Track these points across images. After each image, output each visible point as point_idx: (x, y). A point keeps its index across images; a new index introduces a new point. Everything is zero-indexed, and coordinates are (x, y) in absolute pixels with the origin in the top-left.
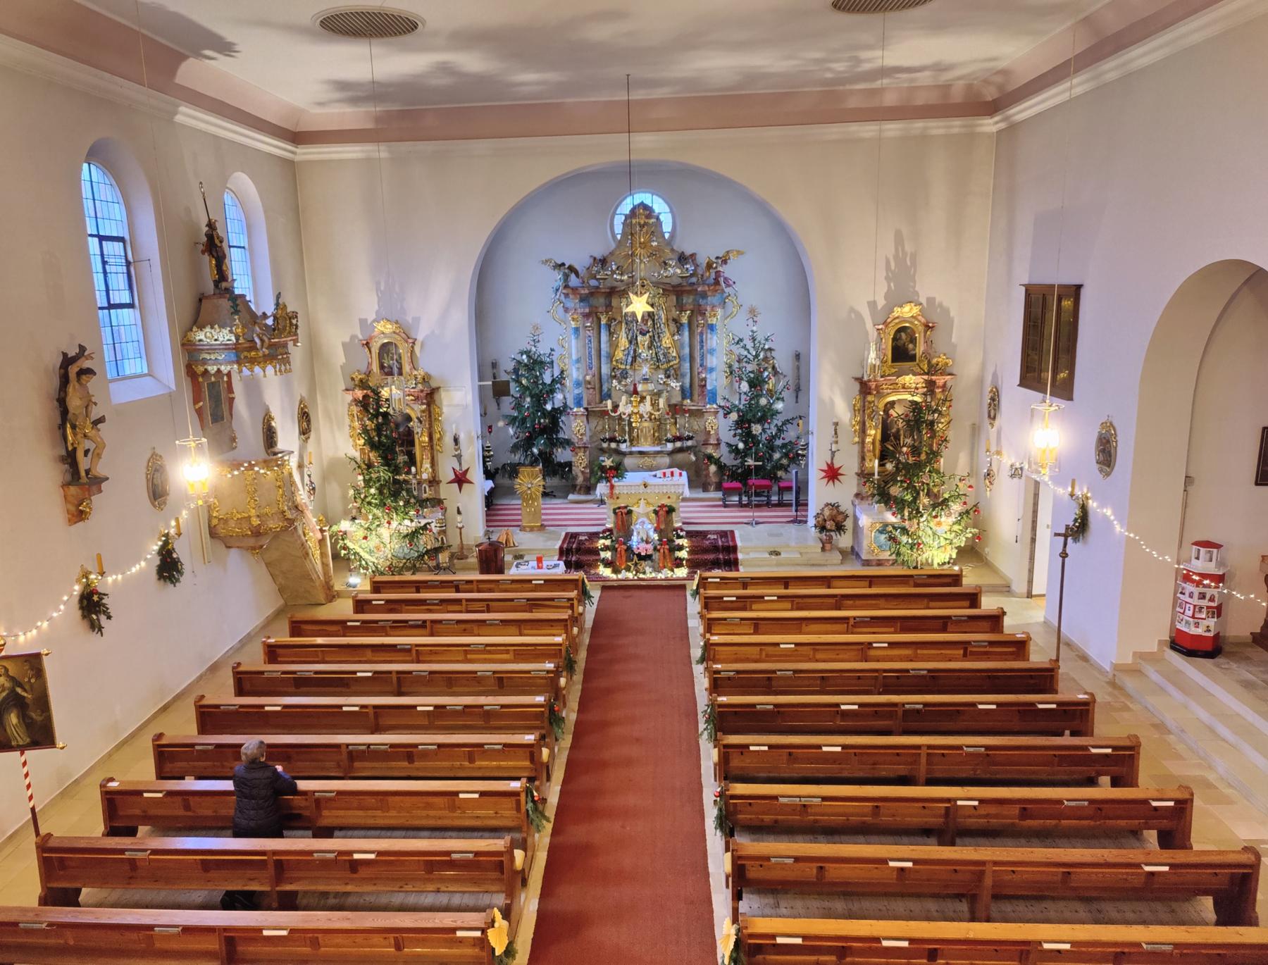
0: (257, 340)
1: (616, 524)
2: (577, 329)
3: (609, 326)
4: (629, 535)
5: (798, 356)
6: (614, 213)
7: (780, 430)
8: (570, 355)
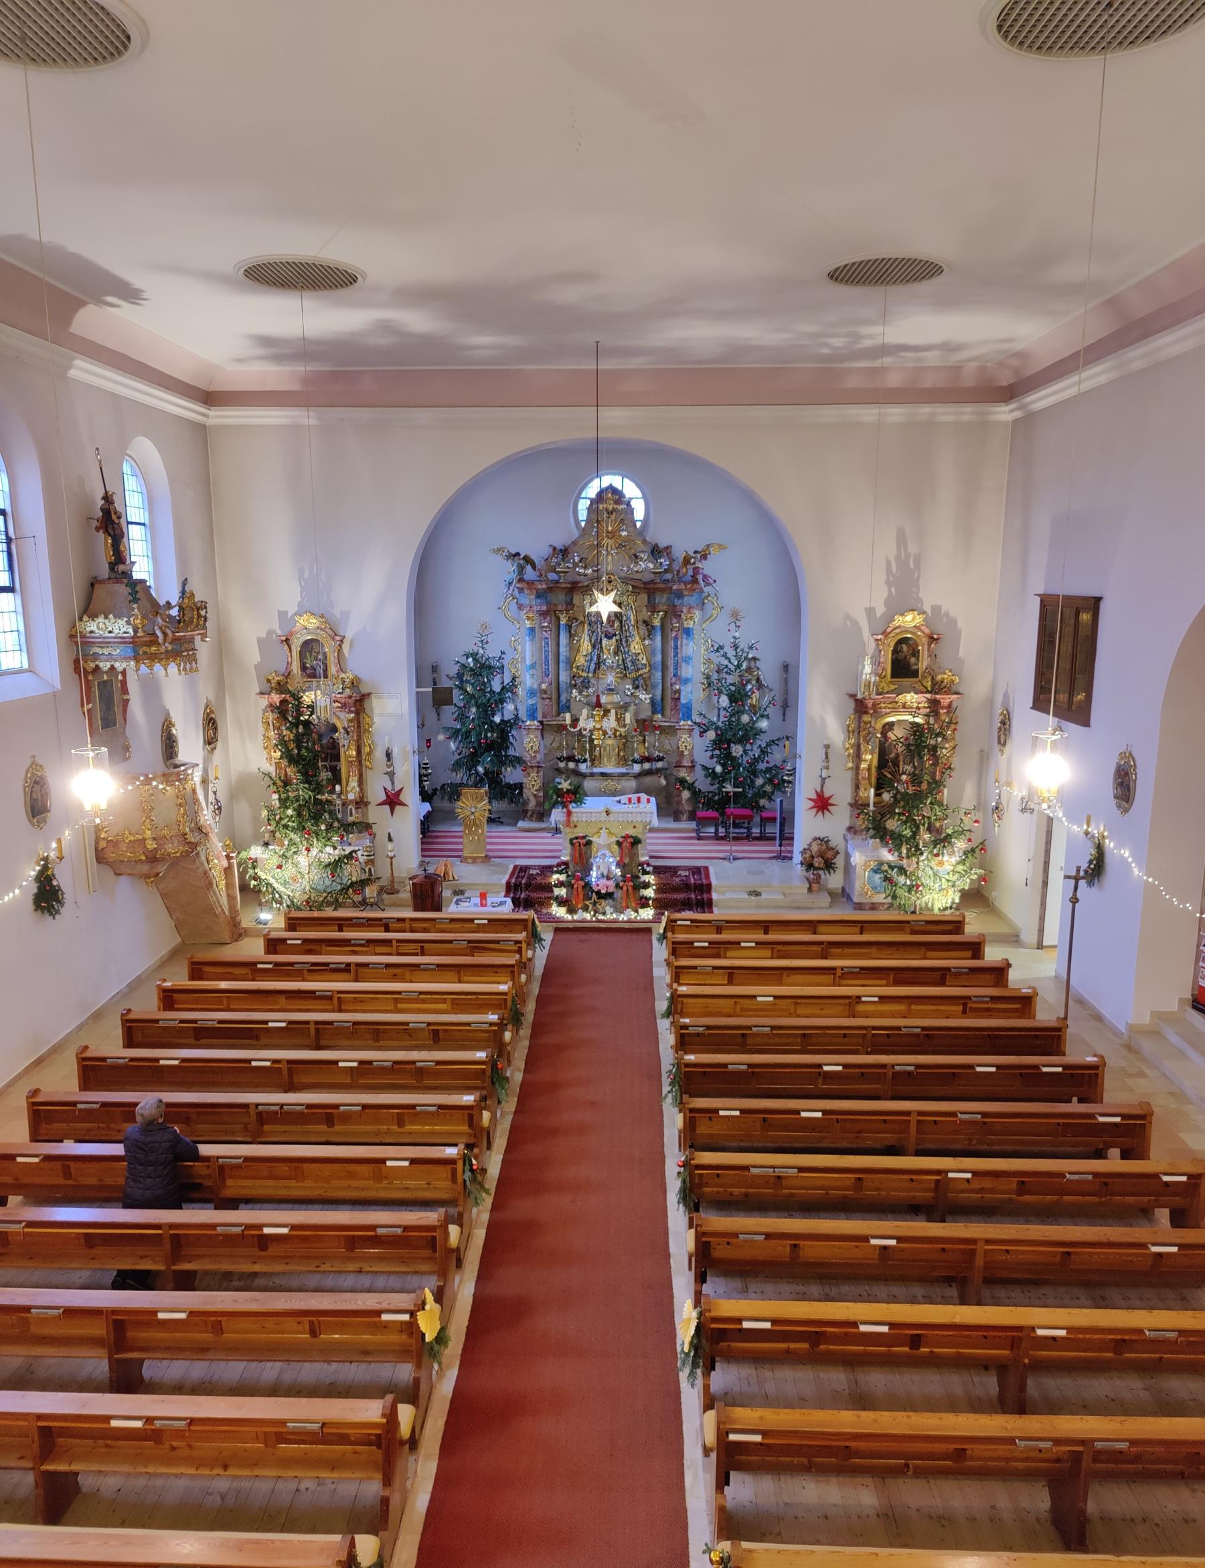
0: (159, 633)
1: (573, 856)
2: (532, 630)
3: (569, 627)
4: (587, 869)
5: (786, 667)
6: (579, 497)
7: (764, 752)
8: (524, 659)
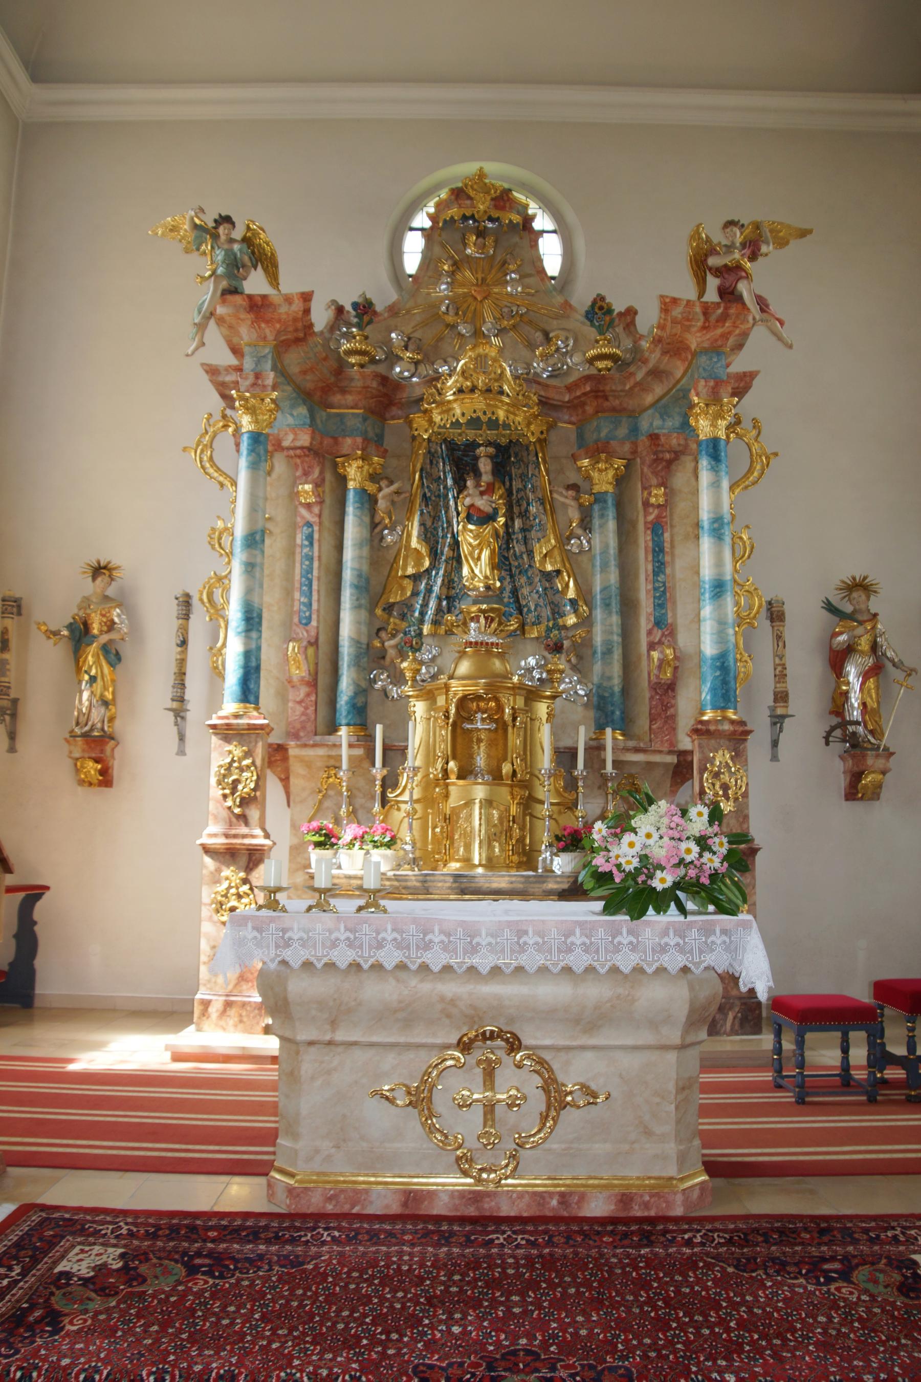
3: (369, 501)
6: (403, 226)
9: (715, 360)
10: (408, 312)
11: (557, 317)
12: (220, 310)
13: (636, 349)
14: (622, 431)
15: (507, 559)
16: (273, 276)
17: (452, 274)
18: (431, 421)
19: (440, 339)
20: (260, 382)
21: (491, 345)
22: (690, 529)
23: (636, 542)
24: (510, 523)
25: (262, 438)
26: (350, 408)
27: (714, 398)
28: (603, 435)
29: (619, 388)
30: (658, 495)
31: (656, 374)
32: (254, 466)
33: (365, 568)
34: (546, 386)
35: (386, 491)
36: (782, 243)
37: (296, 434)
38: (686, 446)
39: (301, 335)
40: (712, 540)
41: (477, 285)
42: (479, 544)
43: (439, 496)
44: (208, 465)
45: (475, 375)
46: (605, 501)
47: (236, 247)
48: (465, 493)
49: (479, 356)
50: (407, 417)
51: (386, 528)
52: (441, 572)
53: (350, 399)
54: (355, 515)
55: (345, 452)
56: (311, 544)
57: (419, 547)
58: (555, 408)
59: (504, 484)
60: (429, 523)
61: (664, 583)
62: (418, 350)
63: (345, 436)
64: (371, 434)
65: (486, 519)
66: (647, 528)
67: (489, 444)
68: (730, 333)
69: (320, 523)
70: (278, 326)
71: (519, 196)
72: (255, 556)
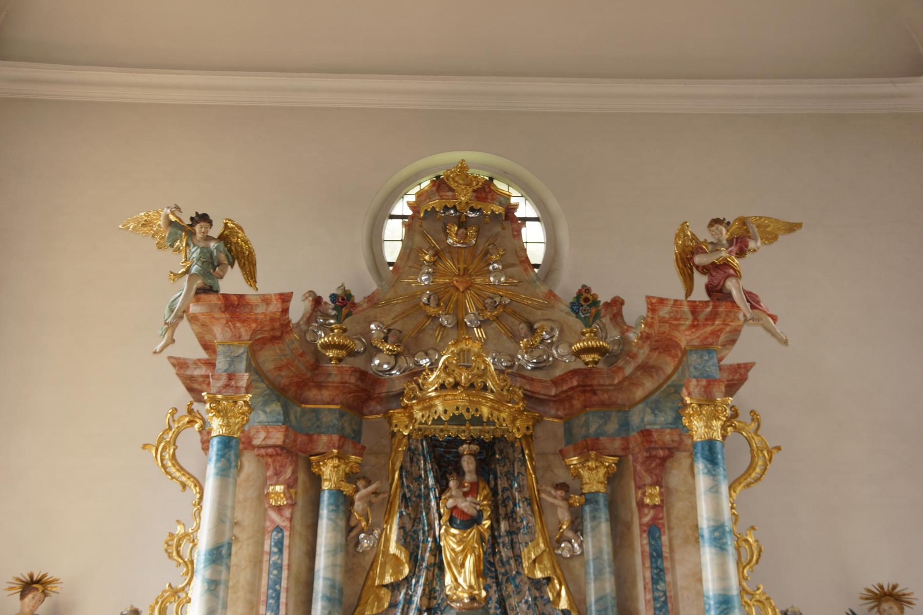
3: (344, 503)
6: (383, 214)
9: (706, 358)
10: (388, 302)
11: (540, 307)
12: (194, 309)
13: (624, 341)
14: (612, 427)
15: (492, 564)
16: (250, 275)
17: (433, 264)
18: (411, 417)
19: (421, 331)
20: (233, 383)
21: (474, 338)
22: (690, 533)
23: (631, 546)
24: (495, 526)
25: (233, 443)
26: (326, 404)
27: (708, 399)
28: (592, 430)
29: (608, 383)
30: (653, 495)
31: (646, 369)
32: (223, 473)
33: (339, 577)
34: (531, 380)
35: (363, 492)
36: (770, 238)
37: (268, 432)
38: (681, 441)
39: (278, 334)
40: (714, 550)
41: (459, 275)
42: (463, 550)
43: (419, 496)
44: (169, 464)
45: (457, 371)
46: (597, 502)
47: (213, 245)
48: (448, 494)
49: (462, 350)
50: (386, 412)
51: (362, 531)
52: (422, 581)
53: (326, 394)
54: (329, 519)
55: (320, 449)
56: (281, 551)
57: (398, 553)
58: (541, 402)
59: (488, 483)
60: (408, 526)
61: (665, 592)
62: (398, 342)
63: (320, 434)
64: (348, 430)
65: (470, 522)
66: (642, 531)
67: (473, 440)
68: (721, 330)
69: (291, 528)
70: (254, 325)
71: (501, 186)
72: (220, 572)
